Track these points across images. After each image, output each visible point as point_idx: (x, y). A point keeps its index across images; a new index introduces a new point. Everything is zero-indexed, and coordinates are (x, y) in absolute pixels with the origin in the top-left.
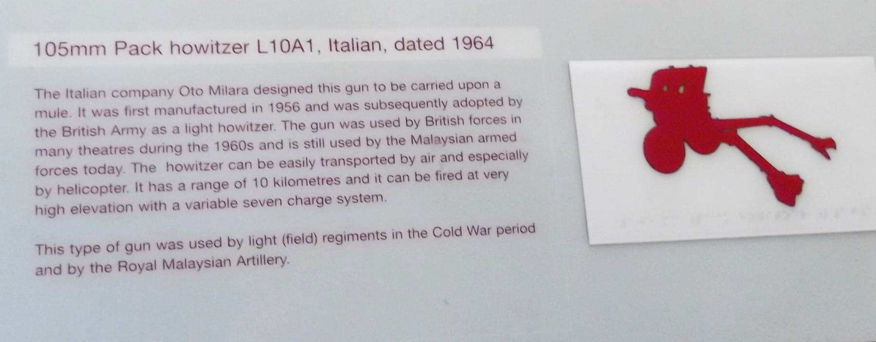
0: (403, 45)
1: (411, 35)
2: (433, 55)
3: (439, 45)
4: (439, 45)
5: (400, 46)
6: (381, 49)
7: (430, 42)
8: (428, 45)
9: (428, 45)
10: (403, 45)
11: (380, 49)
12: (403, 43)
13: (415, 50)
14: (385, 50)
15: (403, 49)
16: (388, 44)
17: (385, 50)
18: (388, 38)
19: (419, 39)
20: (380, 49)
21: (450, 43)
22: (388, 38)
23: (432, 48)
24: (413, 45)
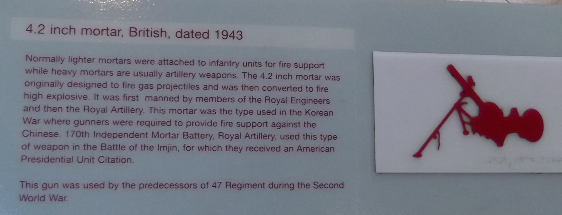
0: (182, 34)
1: (187, 28)
2: (201, 42)
3: (206, 35)
4: (206, 35)
5: (179, 35)
6: (167, 36)
7: (200, 33)
8: (199, 35)
9: (199, 35)
10: (182, 34)
11: (166, 37)
12: (181, 32)
13: (189, 38)
14: (169, 37)
15: (181, 37)
16: (171, 32)
17: (169, 37)
18: (172, 28)
19: (192, 30)
20: (166, 37)
21: (213, 35)
22: (172, 28)
23: (200, 37)
24: (188, 35)
